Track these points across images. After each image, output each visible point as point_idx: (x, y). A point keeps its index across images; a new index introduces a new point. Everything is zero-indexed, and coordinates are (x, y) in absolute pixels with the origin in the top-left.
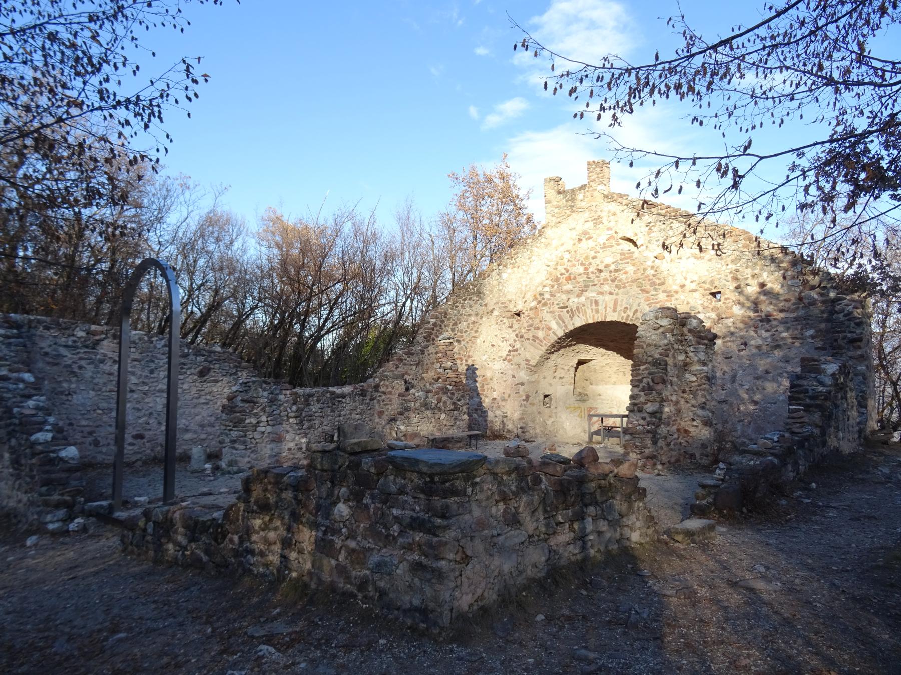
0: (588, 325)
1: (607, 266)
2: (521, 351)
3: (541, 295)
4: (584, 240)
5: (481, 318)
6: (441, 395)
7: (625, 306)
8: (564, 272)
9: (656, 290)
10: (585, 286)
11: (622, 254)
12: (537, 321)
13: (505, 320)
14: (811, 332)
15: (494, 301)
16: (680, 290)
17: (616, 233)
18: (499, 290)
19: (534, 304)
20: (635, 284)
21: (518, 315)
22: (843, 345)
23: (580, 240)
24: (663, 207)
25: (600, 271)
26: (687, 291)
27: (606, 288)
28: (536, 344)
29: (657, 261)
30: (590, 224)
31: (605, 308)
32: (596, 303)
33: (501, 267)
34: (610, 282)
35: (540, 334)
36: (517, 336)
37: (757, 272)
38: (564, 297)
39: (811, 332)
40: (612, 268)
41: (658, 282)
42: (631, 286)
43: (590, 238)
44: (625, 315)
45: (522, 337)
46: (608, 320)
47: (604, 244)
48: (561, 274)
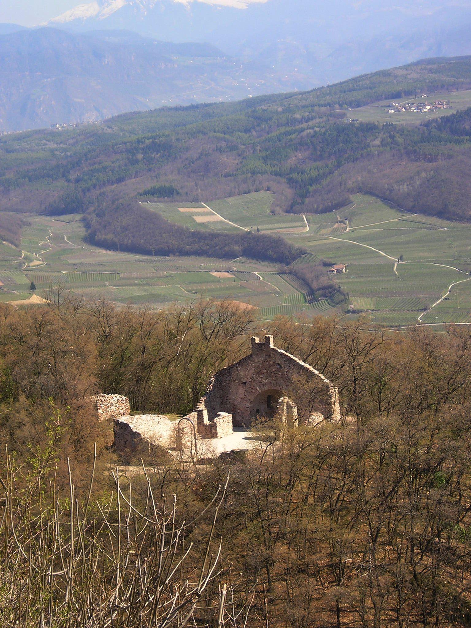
12: (252, 386)
19: (250, 380)
21: (245, 383)
35: (253, 391)
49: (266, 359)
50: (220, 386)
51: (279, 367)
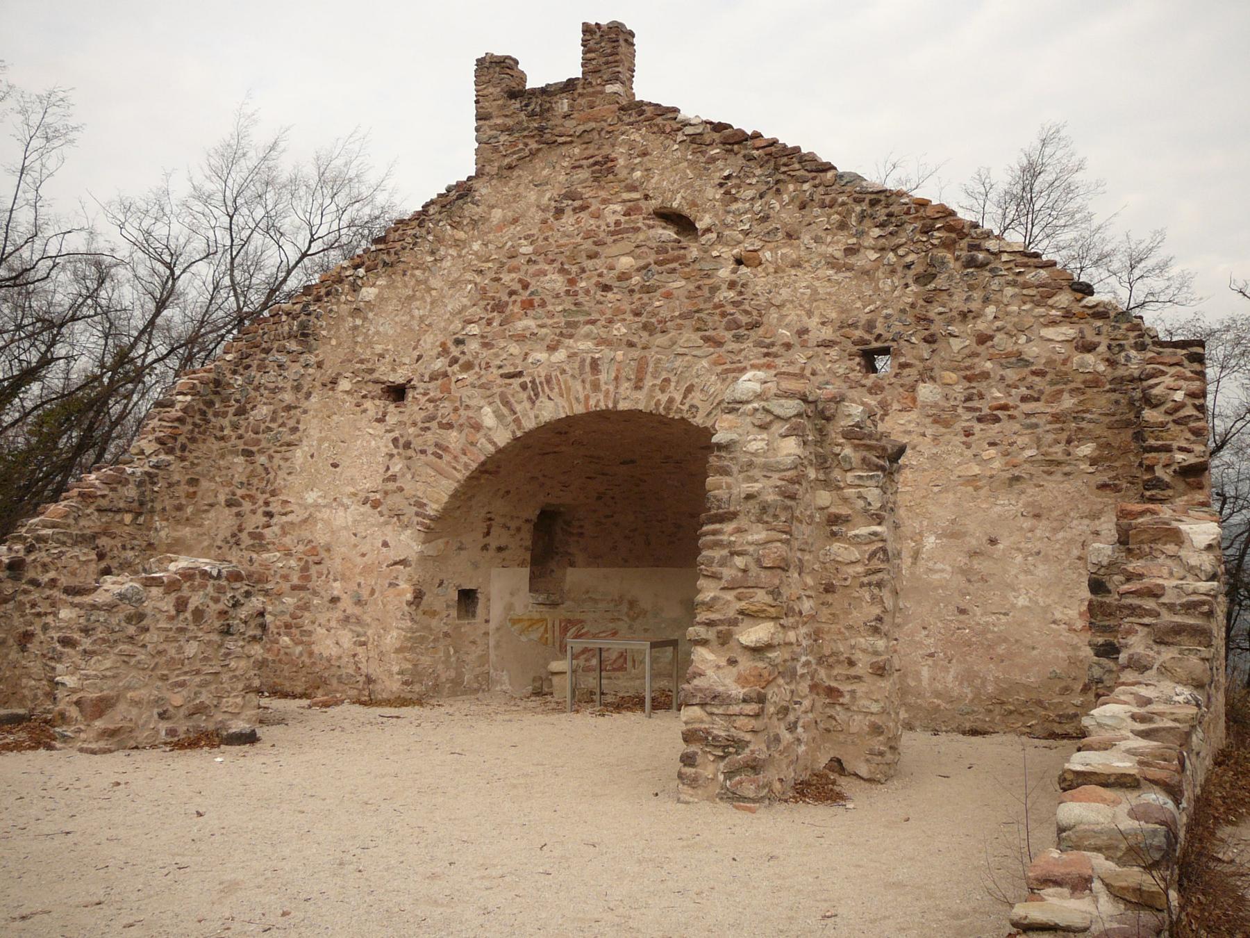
0: (570, 421)
1: (624, 277)
2: (407, 483)
3: (459, 342)
4: (569, 211)
5: (308, 395)
6: (186, 592)
7: (664, 375)
8: (517, 287)
9: (738, 338)
10: (568, 324)
11: (661, 250)
12: (445, 408)
13: (368, 404)
14: (1087, 449)
15: (342, 353)
16: (793, 340)
17: (646, 197)
18: (355, 328)
19: (439, 364)
20: (687, 322)
21: (397, 393)
22: (1167, 479)
23: (559, 212)
24: (758, 143)
25: (606, 288)
26: (813, 342)
27: (619, 330)
28: (441, 464)
29: (744, 269)
30: (584, 174)
31: (616, 378)
32: (595, 365)
33: (361, 271)
34: (629, 317)
36: (395, 440)
37: (974, 306)
38: (514, 349)
39: (1087, 449)
40: (636, 279)
41: (744, 319)
42: (680, 327)
43: (583, 208)
44: (664, 398)
45: (407, 445)
46: (623, 406)
47: (617, 223)
48: (512, 293)
49: (571, 196)
50: (235, 427)
51: (669, 233)
